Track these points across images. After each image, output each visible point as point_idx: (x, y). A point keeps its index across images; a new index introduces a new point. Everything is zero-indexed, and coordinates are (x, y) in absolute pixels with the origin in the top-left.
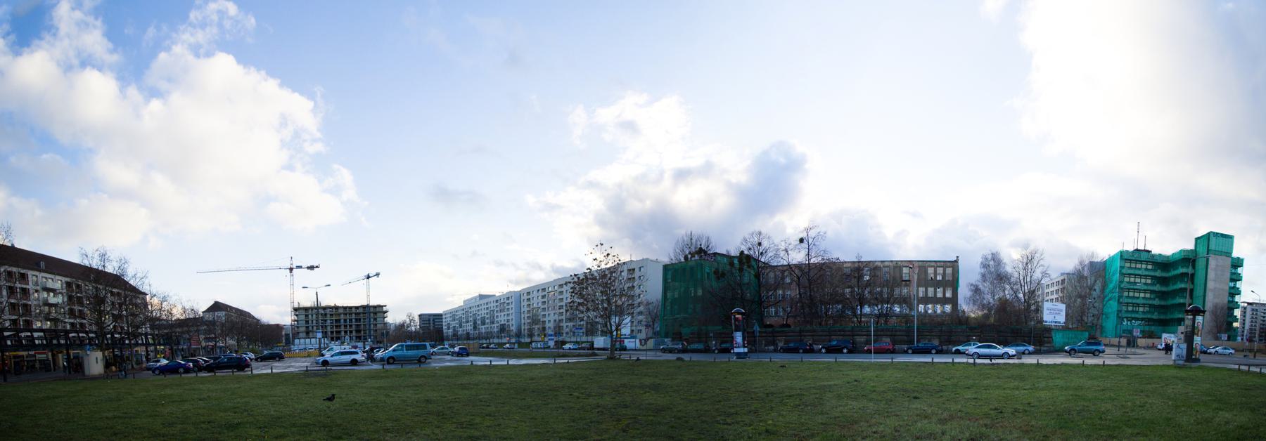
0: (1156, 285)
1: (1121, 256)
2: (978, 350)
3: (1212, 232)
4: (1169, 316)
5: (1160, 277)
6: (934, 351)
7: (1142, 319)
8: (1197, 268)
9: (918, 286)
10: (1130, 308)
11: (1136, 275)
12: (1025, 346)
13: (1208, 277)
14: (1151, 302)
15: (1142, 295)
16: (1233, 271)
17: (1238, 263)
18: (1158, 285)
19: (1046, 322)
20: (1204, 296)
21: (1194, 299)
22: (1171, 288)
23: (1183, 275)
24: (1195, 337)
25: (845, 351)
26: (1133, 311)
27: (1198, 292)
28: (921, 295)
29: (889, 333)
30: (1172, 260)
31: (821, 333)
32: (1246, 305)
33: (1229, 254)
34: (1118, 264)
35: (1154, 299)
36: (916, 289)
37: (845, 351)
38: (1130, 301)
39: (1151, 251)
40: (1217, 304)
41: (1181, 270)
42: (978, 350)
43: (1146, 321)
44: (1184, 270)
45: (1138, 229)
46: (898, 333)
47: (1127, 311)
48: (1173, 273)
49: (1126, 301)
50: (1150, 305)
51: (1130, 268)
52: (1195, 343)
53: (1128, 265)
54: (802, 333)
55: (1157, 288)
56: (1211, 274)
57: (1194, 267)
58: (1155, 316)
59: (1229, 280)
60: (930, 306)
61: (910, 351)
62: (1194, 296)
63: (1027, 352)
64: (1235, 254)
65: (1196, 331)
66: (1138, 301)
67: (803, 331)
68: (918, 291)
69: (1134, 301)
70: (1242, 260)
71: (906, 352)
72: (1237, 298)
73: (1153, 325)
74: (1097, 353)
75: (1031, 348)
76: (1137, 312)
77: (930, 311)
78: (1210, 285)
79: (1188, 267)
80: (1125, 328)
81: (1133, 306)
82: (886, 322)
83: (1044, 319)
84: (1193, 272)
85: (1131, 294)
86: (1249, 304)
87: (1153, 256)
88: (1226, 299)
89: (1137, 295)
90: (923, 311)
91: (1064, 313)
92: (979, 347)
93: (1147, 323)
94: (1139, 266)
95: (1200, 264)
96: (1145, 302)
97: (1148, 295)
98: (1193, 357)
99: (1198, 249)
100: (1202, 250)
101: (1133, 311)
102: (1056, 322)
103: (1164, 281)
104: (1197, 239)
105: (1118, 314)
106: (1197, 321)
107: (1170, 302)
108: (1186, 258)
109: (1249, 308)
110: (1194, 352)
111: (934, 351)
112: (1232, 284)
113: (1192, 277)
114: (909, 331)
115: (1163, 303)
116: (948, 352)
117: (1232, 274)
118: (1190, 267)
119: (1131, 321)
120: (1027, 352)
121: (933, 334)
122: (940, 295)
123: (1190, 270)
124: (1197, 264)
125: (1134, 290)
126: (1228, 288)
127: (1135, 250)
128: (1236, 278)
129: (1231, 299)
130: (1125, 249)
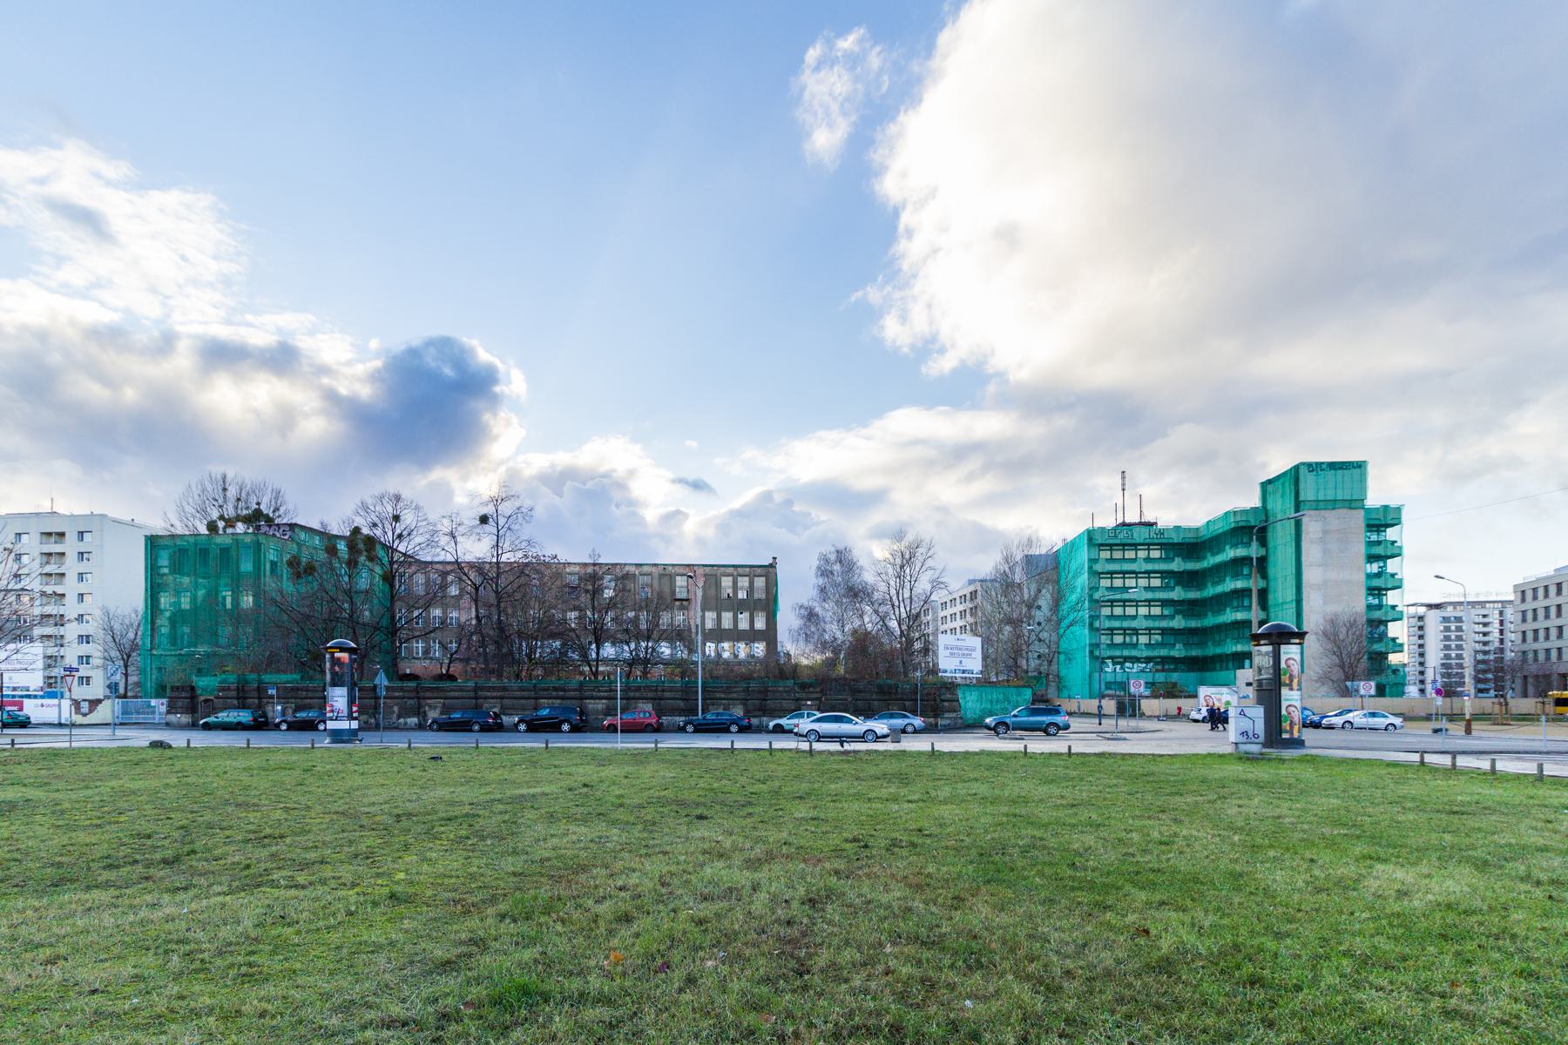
0: (1173, 589)
1: (1090, 539)
2: (816, 726)
3: (1303, 464)
4: (1211, 650)
5: (1183, 572)
6: (734, 728)
8: (1271, 544)
9: (703, 610)
10: (1118, 639)
11: (1124, 573)
12: (905, 716)
13: (1304, 558)
14: (1164, 624)
15: (1143, 611)
16: (1374, 537)
17: (1380, 521)
18: (1178, 589)
19: (945, 671)
20: (1299, 601)
21: (1272, 610)
22: (1211, 591)
24: (1285, 691)
25: (566, 727)
26: (1124, 645)
27: (1282, 592)
28: (709, 625)
29: (650, 695)
30: (1206, 534)
31: (519, 694)
32: (1422, 610)
33: (1355, 503)
34: (1083, 555)
35: (1172, 617)
36: (699, 614)
37: (566, 727)
38: (1116, 624)
39: (1156, 523)
40: (1336, 615)
41: (1230, 553)
42: (816, 726)
43: (1157, 663)
44: (1240, 552)
45: (1123, 484)
46: (667, 694)
47: (1112, 645)
48: (1212, 560)
49: (1107, 624)
51: (1112, 560)
52: (1284, 704)
53: (1105, 554)
54: (481, 693)
55: (1177, 594)
57: (1263, 542)
58: (1178, 651)
59: (1363, 559)
60: (726, 645)
61: (690, 728)
62: (1271, 602)
63: (910, 729)
64: (1374, 499)
65: (1286, 679)
66: (1134, 624)
67: (482, 689)
68: (703, 617)
69: (1126, 624)
70: (1398, 510)
71: (682, 730)
72: (1392, 598)
73: (1175, 670)
74: (1052, 730)
75: (918, 722)
76: (1135, 646)
77: (726, 655)
78: (1311, 575)
79: (1249, 544)
80: (1110, 678)
81: (1125, 634)
82: (645, 673)
83: (941, 666)
84: (1262, 552)
85: (1118, 611)
86: (1430, 606)
87: (1161, 532)
88: (1359, 603)
89: (1130, 611)
90: (713, 654)
91: (978, 654)
92: (819, 720)
94: (1130, 554)
96: (1150, 624)
97: (1156, 611)
98: (1285, 736)
101: (1124, 645)
102: (964, 672)
103: (1191, 579)
105: (1091, 652)
106: (1283, 658)
107: (1210, 621)
109: (1433, 619)
110: (1286, 725)
111: (734, 728)
112: (1374, 568)
113: (1262, 564)
114: (688, 692)
115: (1193, 624)
116: (761, 730)
117: (1370, 544)
118: (1255, 544)
119: (1122, 664)
120: (910, 729)
121: (734, 695)
122: (744, 624)
123: (1254, 551)
124: (1270, 535)
125: (1125, 603)
126: (1363, 577)
127: (1118, 526)
128: (1380, 554)
129: (1376, 602)
130: (1098, 524)
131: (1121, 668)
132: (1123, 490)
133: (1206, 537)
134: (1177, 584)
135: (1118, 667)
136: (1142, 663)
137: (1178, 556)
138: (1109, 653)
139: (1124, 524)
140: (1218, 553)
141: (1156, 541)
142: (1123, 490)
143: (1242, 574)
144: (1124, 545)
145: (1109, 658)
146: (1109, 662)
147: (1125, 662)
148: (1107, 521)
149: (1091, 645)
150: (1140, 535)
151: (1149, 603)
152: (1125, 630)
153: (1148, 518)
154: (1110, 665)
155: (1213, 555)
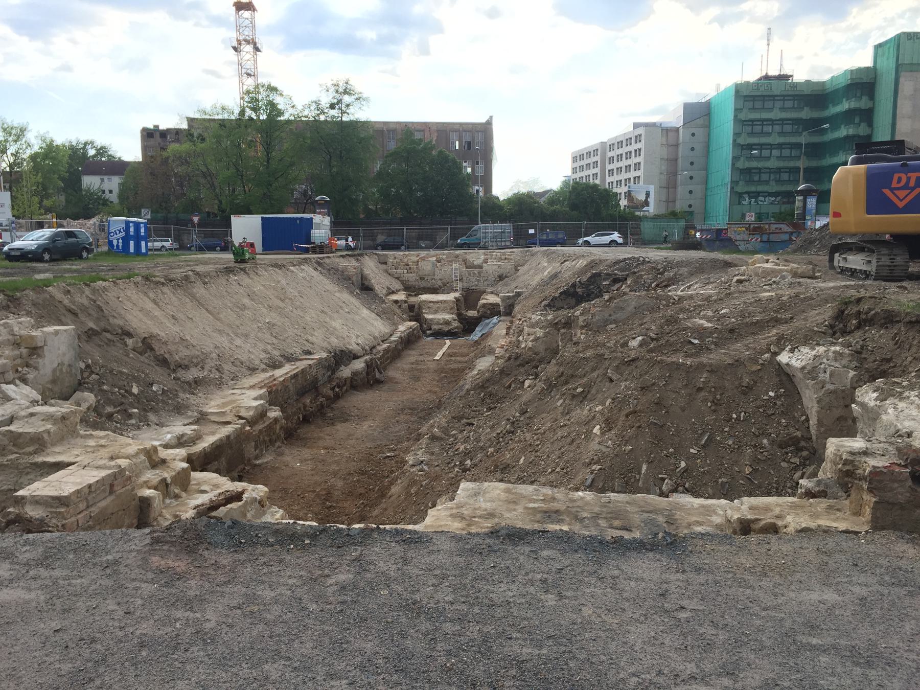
0: (800, 134)
5: (810, 119)
7: (776, 194)
8: (877, 98)
11: (763, 120)
23: (849, 116)
30: (829, 88)
49: (748, 165)
50: (790, 168)
56: (905, 107)
93: (785, 200)
95: (884, 91)
96: (781, 164)
99: (878, 66)
100: (888, 65)
104: (878, 47)
105: (732, 188)
108: (857, 84)
123: (864, 103)
131: (756, 202)
132: (768, 45)
133: (830, 90)
134: (805, 129)
135: (753, 200)
136: (772, 197)
137: (807, 106)
138: (746, 189)
139: (767, 77)
140: (838, 104)
141: (790, 93)
142: (768, 45)
143: (854, 124)
144: (764, 96)
145: (746, 193)
146: (746, 196)
147: (759, 196)
148: (752, 76)
149: (732, 182)
150: (778, 88)
151: (780, 146)
152: (760, 169)
153: (786, 71)
154: (747, 199)
155: (834, 105)
